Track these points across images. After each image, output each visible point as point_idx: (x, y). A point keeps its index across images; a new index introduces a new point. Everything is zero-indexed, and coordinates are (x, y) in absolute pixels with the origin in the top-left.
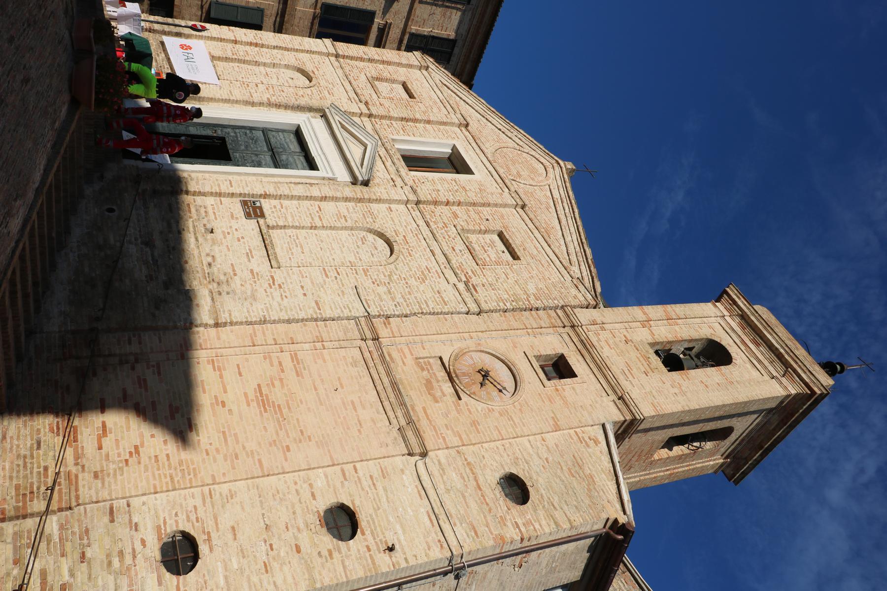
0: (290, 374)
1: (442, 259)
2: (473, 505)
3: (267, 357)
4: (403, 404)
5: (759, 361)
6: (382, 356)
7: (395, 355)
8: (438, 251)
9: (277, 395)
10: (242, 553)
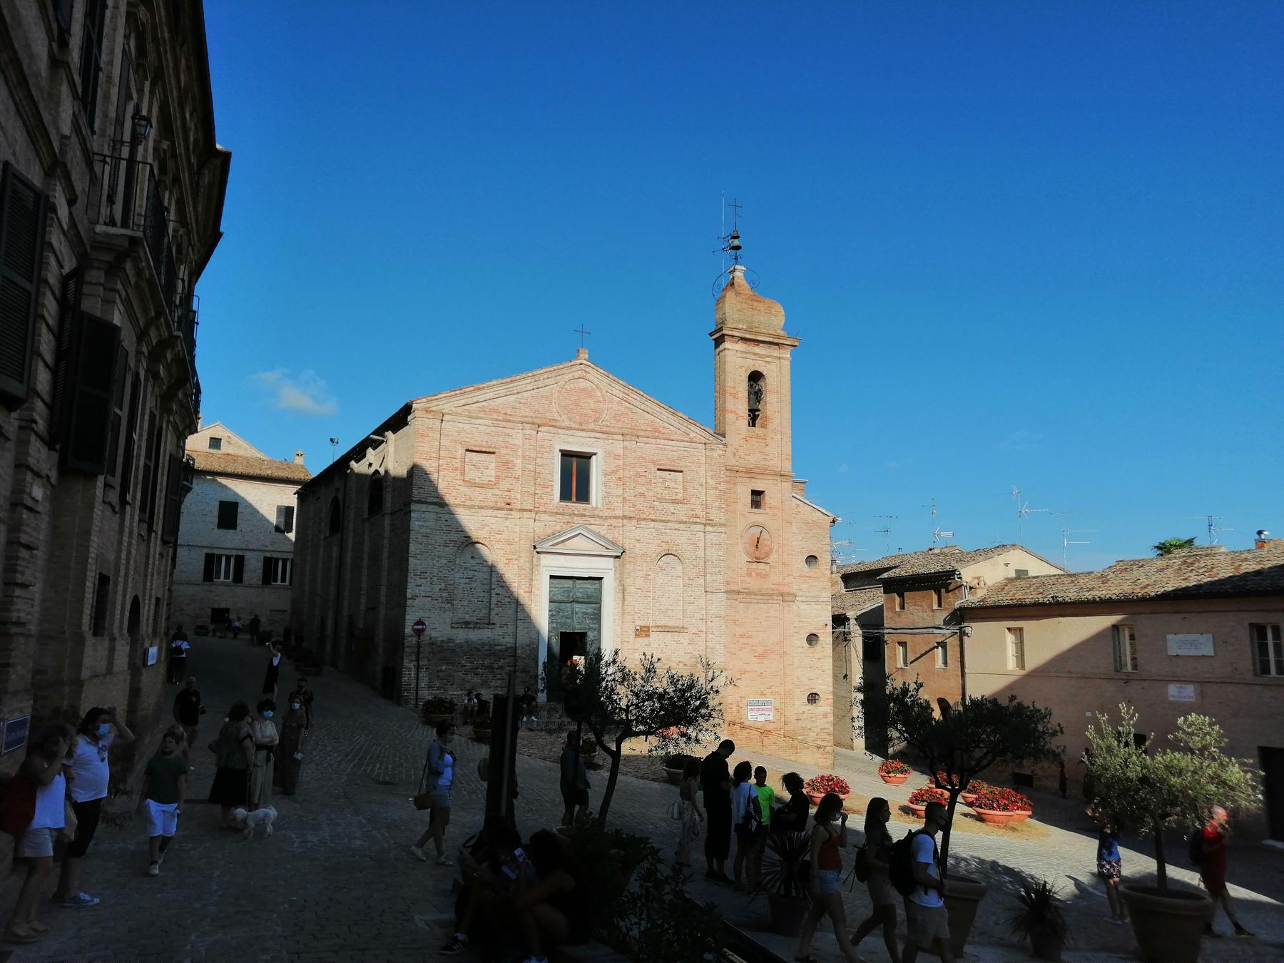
0: (750, 640)
1: (683, 526)
3: (741, 649)
7: (744, 585)
8: (677, 526)
9: (760, 650)
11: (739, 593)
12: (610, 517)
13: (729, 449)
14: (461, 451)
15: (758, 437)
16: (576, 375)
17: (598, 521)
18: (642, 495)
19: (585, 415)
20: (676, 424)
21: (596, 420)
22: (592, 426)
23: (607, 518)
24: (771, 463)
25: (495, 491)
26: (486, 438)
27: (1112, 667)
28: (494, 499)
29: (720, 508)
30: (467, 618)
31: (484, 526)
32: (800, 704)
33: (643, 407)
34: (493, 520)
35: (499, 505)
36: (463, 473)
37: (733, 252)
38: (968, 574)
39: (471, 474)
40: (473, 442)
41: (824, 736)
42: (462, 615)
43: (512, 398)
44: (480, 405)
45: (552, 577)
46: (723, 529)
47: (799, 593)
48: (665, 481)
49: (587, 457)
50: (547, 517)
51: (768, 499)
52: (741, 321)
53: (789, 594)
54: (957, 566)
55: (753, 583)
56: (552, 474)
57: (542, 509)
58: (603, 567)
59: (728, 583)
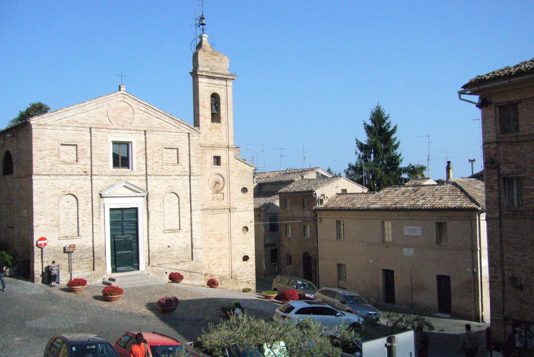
2: (246, 202)
4: (225, 209)
5: (221, 85)
6: (212, 209)
7: (211, 205)
8: (175, 177)
10: (247, 248)
11: (208, 209)
12: (140, 175)
13: (202, 135)
14: (57, 145)
15: (216, 128)
16: (119, 99)
17: (134, 178)
18: (157, 162)
19: (126, 121)
20: (173, 124)
21: (131, 124)
22: (129, 127)
23: (138, 176)
24: (224, 141)
25: (77, 166)
26: (71, 137)
27: (381, 241)
28: (78, 170)
29: (198, 167)
30: (67, 234)
31: (73, 185)
32: (239, 262)
33: (156, 115)
34: (77, 181)
35: (80, 173)
36: (59, 157)
37: (201, 26)
38: (318, 193)
39: (64, 157)
40: (64, 140)
41: (251, 276)
42: (63, 233)
43: (84, 114)
44: (67, 119)
45: (111, 209)
46: (199, 178)
47: (238, 207)
48: (168, 154)
49: (127, 144)
50: (106, 178)
51: (223, 160)
52: (207, 67)
53: (233, 208)
54: (313, 188)
55: (215, 204)
56: (108, 155)
57: (103, 173)
58: (138, 202)
59: (202, 205)
